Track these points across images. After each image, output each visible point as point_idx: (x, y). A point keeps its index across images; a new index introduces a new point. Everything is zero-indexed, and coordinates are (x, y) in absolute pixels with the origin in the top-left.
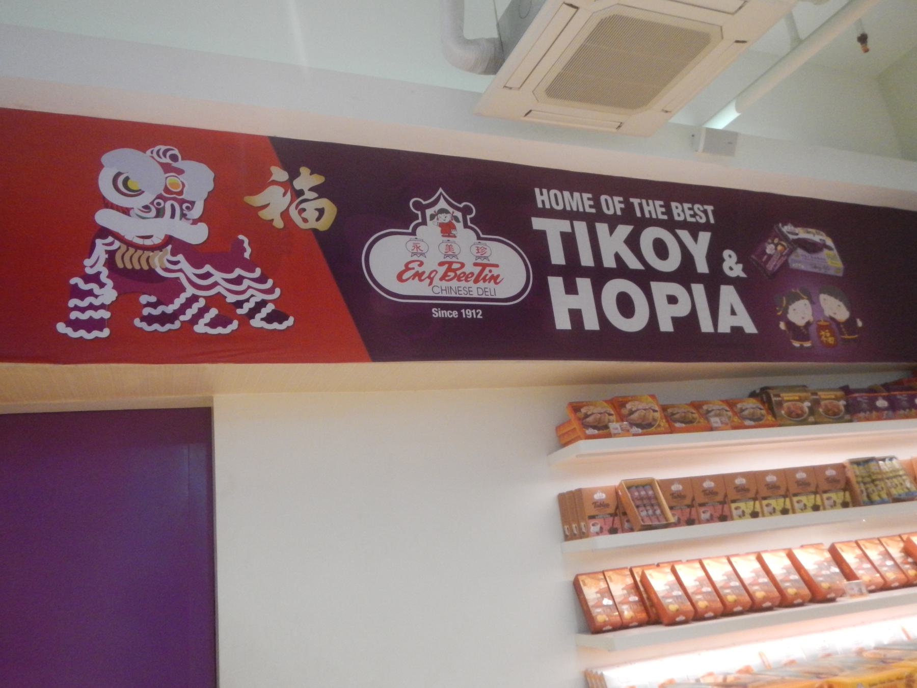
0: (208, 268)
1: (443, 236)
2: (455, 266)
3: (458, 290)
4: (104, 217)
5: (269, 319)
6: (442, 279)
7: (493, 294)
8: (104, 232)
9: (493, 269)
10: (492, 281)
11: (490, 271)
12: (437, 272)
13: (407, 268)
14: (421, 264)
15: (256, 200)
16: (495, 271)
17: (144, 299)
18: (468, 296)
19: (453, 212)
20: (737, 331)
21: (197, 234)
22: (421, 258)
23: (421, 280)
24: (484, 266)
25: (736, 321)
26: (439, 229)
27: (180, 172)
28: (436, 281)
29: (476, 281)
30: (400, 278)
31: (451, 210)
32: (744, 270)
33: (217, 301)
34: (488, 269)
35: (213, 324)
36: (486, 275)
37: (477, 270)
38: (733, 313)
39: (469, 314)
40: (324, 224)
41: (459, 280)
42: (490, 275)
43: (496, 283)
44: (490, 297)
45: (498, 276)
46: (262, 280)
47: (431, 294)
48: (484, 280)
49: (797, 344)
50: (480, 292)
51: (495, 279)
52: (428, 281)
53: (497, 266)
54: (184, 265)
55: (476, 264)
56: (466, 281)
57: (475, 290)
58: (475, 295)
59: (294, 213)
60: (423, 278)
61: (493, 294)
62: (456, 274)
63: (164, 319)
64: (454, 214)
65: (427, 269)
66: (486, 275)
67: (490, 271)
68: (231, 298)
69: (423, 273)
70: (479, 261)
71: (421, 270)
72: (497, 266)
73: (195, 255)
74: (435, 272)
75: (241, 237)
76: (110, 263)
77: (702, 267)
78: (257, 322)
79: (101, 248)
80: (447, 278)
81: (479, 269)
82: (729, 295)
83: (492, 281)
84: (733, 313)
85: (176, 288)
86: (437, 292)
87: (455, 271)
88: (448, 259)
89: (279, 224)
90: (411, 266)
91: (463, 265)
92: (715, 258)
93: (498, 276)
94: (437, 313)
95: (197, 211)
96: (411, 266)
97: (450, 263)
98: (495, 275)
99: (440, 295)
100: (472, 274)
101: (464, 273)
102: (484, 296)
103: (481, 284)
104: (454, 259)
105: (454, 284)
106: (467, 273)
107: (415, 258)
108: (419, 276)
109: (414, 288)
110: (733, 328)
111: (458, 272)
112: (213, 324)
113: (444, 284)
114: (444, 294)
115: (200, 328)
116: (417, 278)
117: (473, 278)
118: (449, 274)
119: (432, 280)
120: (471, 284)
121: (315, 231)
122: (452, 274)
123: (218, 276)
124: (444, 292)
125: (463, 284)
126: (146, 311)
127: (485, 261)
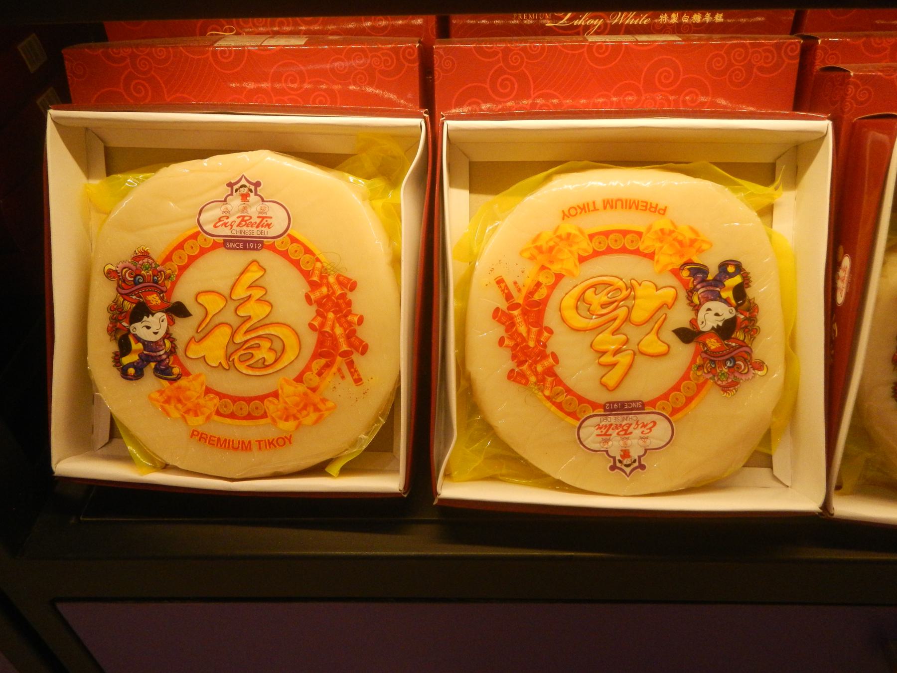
1: (242, 201)
2: (246, 218)
3: (245, 233)
7: (266, 234)
9: (268, 219)
10: (267, 227)
11: (267, 221)
12: (235, 222)
13: (220, 220)
14: (228, 218)
16: (269, 221)
18: (251, 235)
19: (250, 186)
22: (228, 215)
23: (226, 227)
24: (263, 218)
26: (240, 197)
28: (234, 227)
29: (257, 227)
30: (215, 226)
31: (248, 185)
34: (265, 220)
36: (264, 224)
37: (258, 221)
41: (247, 226)
42: (266, 223)
43: (269, 228)
44: (264, 236)
45: (271, 223)
47: (230, 234)
48: (262, 226)
50: (259, 233)
51: (269, 226)
52: (230, 227)
53: (271, 218)
55: (258, 217)
56: (252, 227)
58: (255, 235)
60: (227, 225)
61: (266, 234)
62: (246, 223)
64: (250, 188)
65: (230, 220)
66: (264, 224)
67: (267, 221)
69: (228, 222)
70: (261, 215)
71: (226, 221)
72: (271, 218)
74: (234, 223)
80: (241, 225)
81: (261, 219)
83: (267, 227)
86: (235, 233)
87: (246, 221)
88: (243, 214)
90: (222, 219)
91: (251, 218)
93: (271, 223)
96: (222, 219)
97: (244, 217)
98: (269, 223)
99: (235, 235)
100: (256, 223)
101: (251, 222)
102: (260, 235)
103: (260, 229)
104: (246, 214)
105: (245, 228)
106: (253, 222)
107: (224, 214)
108: (225, 225)
111: (248, 222)
113: (239, 229)
114: (238, 234)
116: (224, 225)
117: (256, 225)
118: (242, 223)
119: (232, 226)
120: (254, 228)
122: (244, 223)
124: (238, 233)
125: (250, 228)
127: (264, 215)
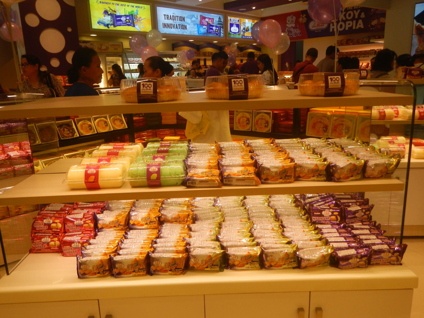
0: (295, 29)
4: (287, 25)
5: (299, 35)
6: (317, 26)
8: (287, 27)
15: (299, 20)
17: (290, 34)
20: (360, 28)
21: (294, 25)
25: (360, 26)
27: (293, 18)
30: (312, 27)
32: (365, 16)
33: (295, 33)
35: (295, 36)
38: (360, 25)
39: (319, 31)
40: (305, 22)
46: (299, 30)
49: (371, 29)
54: (293, 29)
57: (321, 27)
59: (303, 21)
63: (291, 36)
65: (315, 26)
68: (296, 33)
73: (294, 28)
75: (298, 25)
76: (287, 30)
77: (356, 17)
78: (298, 35)
79: (287, 29)
82: (360, 21)
84: (360, 25)
85: (292, 32)
89: (301, 22)
92: (360, 14)
94: (316, 31)
95: (294, 23)
103: (322, 26)
105: (318, 27)
108: (314, 27)
109: (314, 28)
110: (359, 28)
112: (295, 36)
115: (294, 36)
121: (304, 23)
123: (295, 30)
126: (290, 35)
